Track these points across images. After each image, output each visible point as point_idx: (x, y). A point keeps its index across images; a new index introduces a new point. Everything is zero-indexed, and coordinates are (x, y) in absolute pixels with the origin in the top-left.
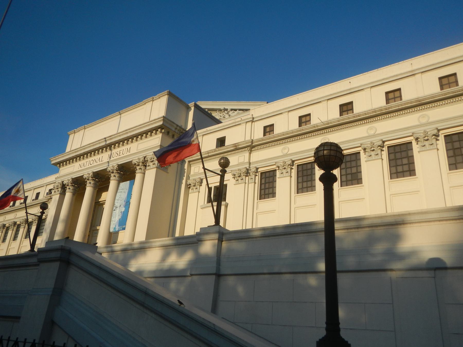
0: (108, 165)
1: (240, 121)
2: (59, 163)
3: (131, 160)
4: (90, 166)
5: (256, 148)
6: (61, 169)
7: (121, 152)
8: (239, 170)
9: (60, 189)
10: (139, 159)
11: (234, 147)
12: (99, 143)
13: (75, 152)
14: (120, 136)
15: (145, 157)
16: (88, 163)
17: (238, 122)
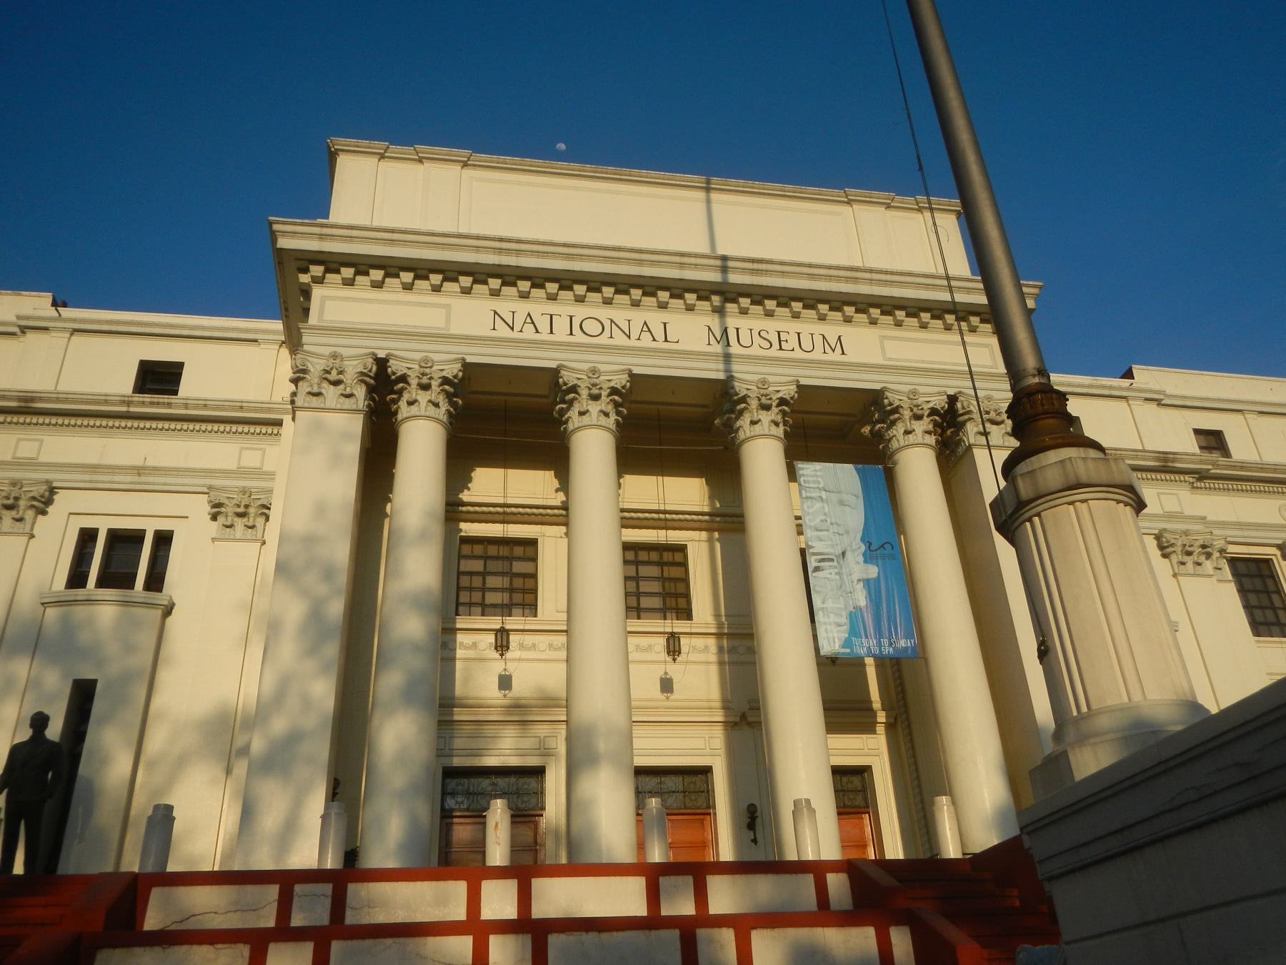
0: (728, 371)
1: (1128, 389)
2: (332, 263)
3: (877, 387)
4: (579, 337)
5: (1208, 483)
6: (317, 292)
7: (793, 342)
8: (1186, 533)
9: (361, 392)
10: (913, 394)
11: (1158, 459)
12: (682, 266)
13: (500, 251)
14: (811, 277)
15: (952, 399)
16: (561, 325)
17: (1120, 388)
